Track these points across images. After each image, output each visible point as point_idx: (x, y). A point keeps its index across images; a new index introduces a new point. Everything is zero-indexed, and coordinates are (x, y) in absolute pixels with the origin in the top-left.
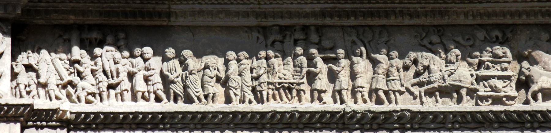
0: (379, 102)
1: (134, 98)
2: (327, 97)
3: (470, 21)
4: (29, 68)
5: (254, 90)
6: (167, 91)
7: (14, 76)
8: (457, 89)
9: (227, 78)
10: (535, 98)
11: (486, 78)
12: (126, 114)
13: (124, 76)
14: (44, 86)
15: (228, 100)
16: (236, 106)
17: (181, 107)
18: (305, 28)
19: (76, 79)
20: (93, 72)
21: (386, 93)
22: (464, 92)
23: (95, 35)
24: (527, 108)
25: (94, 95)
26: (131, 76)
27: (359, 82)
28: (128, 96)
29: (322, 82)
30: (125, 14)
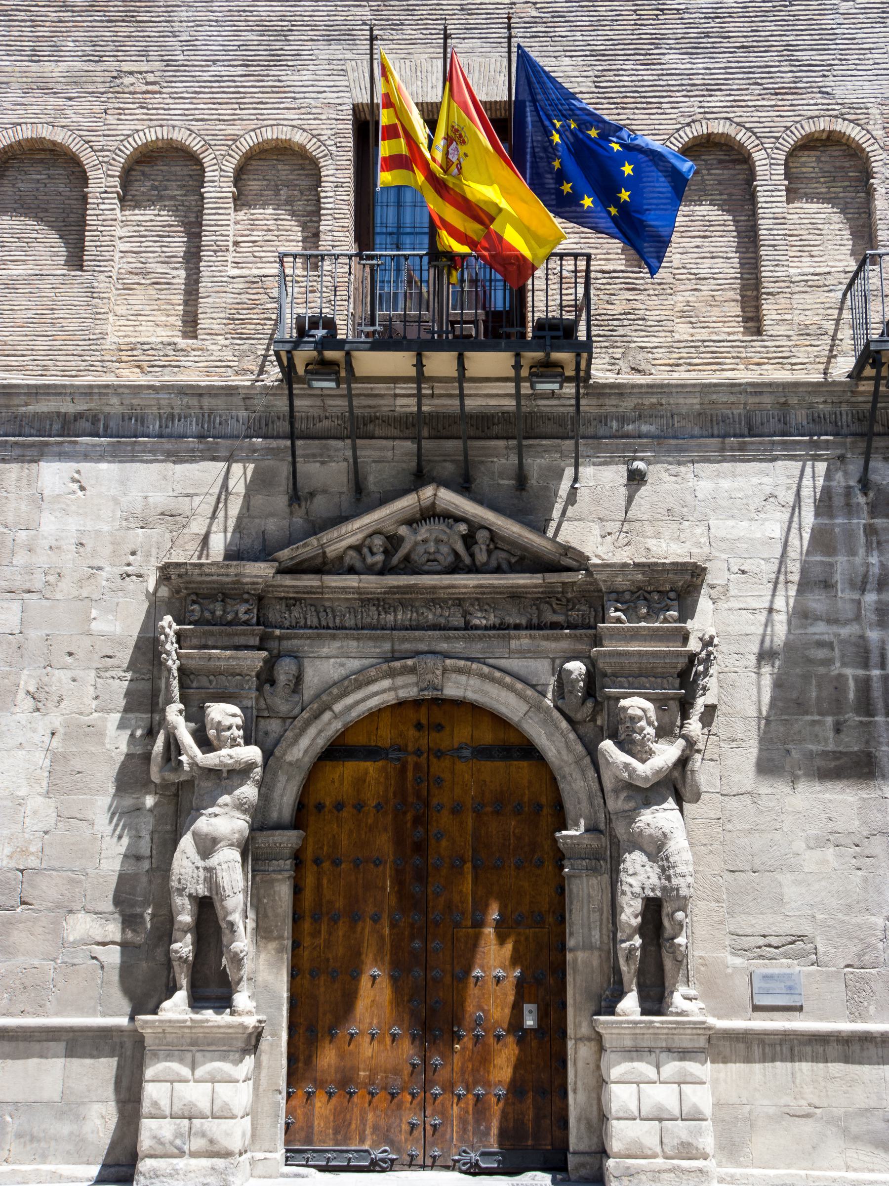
18: (378, 599)
30: (304, 593)
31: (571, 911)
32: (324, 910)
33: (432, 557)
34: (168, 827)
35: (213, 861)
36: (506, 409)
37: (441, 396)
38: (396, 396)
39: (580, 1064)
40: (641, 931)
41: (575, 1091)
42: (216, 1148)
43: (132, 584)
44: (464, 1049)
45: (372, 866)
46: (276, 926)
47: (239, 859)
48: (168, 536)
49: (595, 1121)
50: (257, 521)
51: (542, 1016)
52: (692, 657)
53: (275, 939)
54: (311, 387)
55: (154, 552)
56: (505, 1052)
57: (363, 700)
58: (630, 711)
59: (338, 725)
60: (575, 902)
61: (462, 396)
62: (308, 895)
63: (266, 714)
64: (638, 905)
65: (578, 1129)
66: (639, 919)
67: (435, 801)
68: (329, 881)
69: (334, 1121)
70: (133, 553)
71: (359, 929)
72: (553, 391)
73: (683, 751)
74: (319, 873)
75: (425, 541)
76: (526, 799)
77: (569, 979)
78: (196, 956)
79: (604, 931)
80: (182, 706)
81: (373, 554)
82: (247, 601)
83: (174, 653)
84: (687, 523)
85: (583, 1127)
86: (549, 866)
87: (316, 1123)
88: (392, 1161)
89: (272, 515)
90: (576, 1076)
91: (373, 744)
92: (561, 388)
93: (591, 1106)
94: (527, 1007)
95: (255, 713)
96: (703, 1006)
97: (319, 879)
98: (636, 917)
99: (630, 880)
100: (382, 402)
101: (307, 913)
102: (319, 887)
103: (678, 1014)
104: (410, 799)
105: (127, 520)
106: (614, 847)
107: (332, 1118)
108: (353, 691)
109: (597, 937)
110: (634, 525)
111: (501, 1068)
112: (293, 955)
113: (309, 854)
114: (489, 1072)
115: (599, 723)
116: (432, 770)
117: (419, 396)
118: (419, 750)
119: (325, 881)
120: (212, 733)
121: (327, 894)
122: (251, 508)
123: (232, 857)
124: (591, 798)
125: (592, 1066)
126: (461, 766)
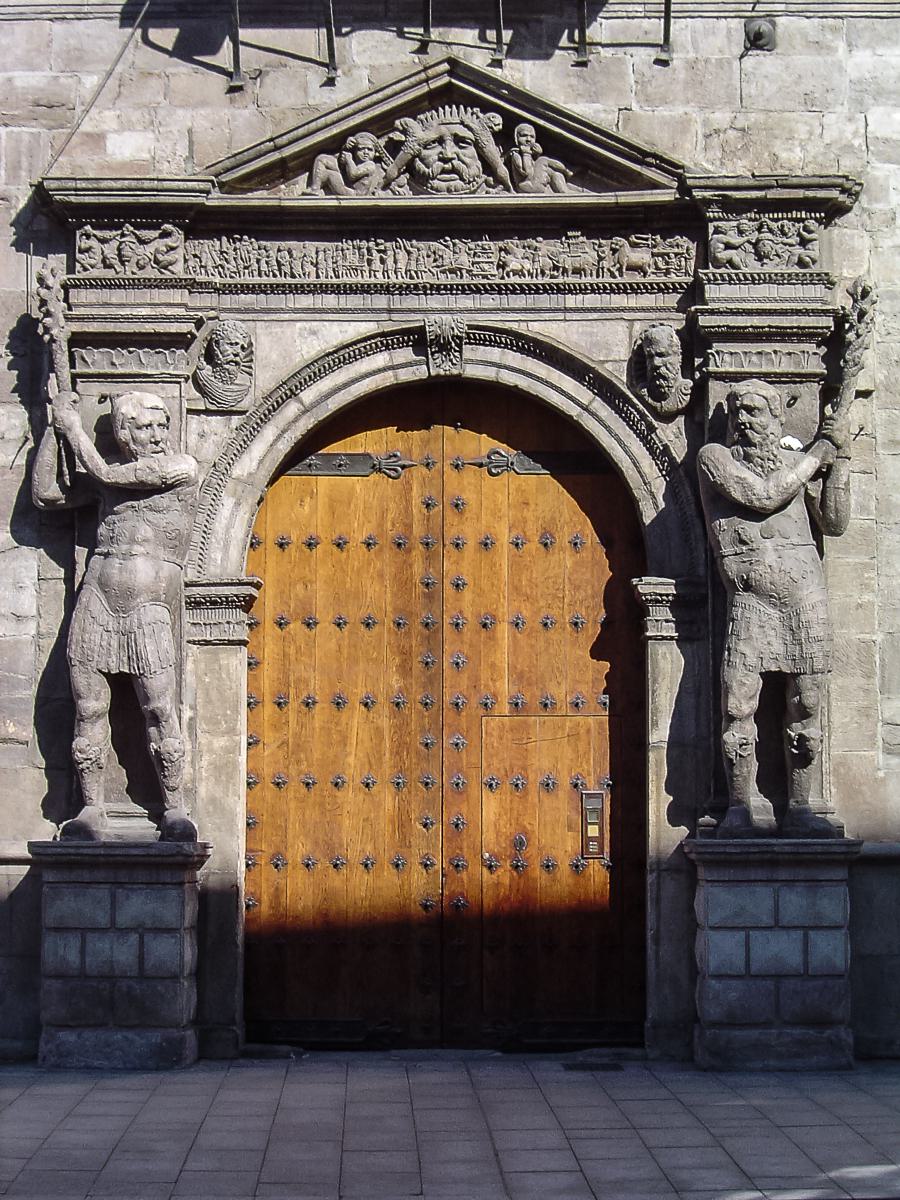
0: (411, 278)
1: (260, 275)
2: (379, 275)
3: (469, 227)
6: (280, 270)
7: (186, 261)
8: (460, 270)
9: (317, 263)
10: (508, 276)
11: (478, 263)
13: (253, 261)
14: (205, 267)
15: (318, 277)
16: (323, 280)
17: (289, 280)
20: (235, 259)
21: (416, 272)
22: (464, 272)
24: (503, 282)
25: (235, 273)
26: (258, 261)
27: (399, 265)
28: (256, 273)
29: (377, 265)
33: (448, 166)
40: (759, 716)
41: (657, 941)
46: (226, 715)
52: (841, 319)
53: (223, 734)
55: (25, 164)
57: (346, 385)
62: (268, 673)
64: (755, 683)
67: (451, 534)
73: (823, 459)
75: (441, 141)
81: (358, 161)
82: (166, 235)
84: (833, 116)
89: (204, 103)
90: (658, 917)
120: (124, 435)
123: (158, 617)
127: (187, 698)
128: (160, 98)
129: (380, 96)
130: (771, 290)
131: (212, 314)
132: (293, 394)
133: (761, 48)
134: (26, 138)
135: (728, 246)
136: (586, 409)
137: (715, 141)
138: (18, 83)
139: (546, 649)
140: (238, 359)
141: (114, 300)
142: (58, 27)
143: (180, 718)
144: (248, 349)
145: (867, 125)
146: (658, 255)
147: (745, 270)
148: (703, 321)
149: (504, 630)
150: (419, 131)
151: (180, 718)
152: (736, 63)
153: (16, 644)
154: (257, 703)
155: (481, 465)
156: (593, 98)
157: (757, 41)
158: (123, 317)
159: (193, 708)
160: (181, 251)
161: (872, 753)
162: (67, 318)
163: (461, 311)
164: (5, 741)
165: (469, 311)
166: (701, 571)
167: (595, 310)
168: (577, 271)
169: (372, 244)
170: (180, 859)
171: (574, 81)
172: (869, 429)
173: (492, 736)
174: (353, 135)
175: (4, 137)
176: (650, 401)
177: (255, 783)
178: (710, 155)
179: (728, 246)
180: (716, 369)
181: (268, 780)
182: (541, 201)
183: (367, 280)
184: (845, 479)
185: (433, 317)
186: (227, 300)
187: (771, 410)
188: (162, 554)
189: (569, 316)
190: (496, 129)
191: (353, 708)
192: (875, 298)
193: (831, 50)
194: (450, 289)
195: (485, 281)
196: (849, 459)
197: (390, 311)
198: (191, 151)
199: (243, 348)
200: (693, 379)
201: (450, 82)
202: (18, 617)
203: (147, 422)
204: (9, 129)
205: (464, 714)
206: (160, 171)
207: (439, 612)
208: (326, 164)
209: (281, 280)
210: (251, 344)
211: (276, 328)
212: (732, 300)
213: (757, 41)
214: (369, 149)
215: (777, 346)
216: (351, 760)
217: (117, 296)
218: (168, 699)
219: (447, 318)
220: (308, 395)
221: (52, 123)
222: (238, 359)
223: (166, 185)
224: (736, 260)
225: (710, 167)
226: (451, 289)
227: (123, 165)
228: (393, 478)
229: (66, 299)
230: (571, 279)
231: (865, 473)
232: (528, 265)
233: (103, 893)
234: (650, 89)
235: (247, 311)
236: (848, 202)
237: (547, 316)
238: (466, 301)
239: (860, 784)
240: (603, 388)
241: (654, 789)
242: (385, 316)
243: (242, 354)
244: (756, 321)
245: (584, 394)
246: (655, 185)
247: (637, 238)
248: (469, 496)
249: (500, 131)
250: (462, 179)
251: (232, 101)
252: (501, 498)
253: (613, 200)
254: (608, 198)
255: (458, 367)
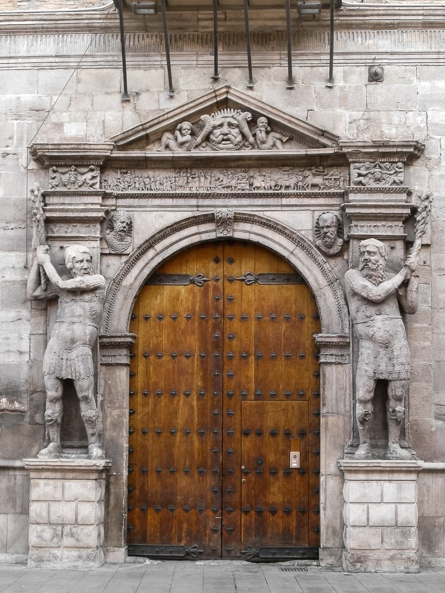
4: (105, 180)
5: (171, 187)
6: (145, 187)
7: (101, 183)
8: (231, 186)
10: (254, 189)
11: (240, 183)
12: (133, 194)
19: (119, 184)
22: (233, 187)
23: (125, 171)
31: (324, 389)
32: (151, 389)
33: (226, 137)
34: (41, 332)
35: (73, 354)
36: (279, 29)
37: (230, 20)
38: (199, 20)
39: (329, 492)
40: (373, 400)
41: (325, 509)
42: (81, 544)
43: (9, 161)
44: (248, 481)
45: (184, 359)
46: (118, 399)
47: (90, 353)
48: (35, 126)
49: (338, 528)
50: (99, 113)
51: (304, 459)
52: (414, 210)
53: (117, 408)
54: (136, 14)
56: (277, 484)
58: (368, 249)
59: (159, 259)
60: (327, 383)
61: (247, 20)
63: (107, 251)
64: (372, 384)
65: (327, 533)
66: (372, 394)
68: (154, 368)
69: (161, 528)
70: (10, 138)
71: (175, 402)
72: (314, 15)
73: (406, 277)
74: (147, 363)
75: (221, 125)
76: (293, 311)
77: (322, 435)
78: (63, 419)
79: (347, 403)
80: (47, 247)
81: (183, 135)
82: (92, 170)
83: (41, 209)
85: (330, 532)
86: (309, 359)
87: (148, 529)
88: (200, 553)
89: (110, 108)
91: (184, 273)
92: (320, 12)
93: (336, 518)
94: (292, 454)
95: (99, 251)
96: (415, 453)
97: (147, 367)
98: (370, 392)
99: (365, 367)
100: (188, 24)
101: (140, 390)
102: (147, 373)
103: (397, 458)
104: (211, 312)
105: (6, 114)
106: (355, 345)
107: (159, 526)
108: (170, 234)
109: (342, 407)
110: (372, 114)
111: (274, 494)
112: (130, 420)
113: (140, 350)
114: (266, 497)
115: (345, 257)
116: (226, 291)
117: (215, 19)
118: (216, 276)
119: (151, 368)
121: (153, 379)
122: (94, 104)
124: (339, 310)
125: (337, 492)
126: (246, 288)
127: (101, 390)
128: (90, 106)
129: (193, 104)
130: (381, 196)
131: (114, 208)
132: (151, 246)
133: (376, 81)
134: (26, 125)
135: (360, 175)
136: (292, 253)
137: (354, 125)
138: (22, 100)
139: (273, 368)
140: (125, 229)
141: (66, 202)
142: (41, 73)
143: (96, 401)
144: (130, 225)
145: (427, 117)
146: (326, 179)
147: (368, 186)
148: (348, 211)
149: (252, 358)
150: (210, 120)
151: (96, 401)
152: (365, 88)
153: (19, 366)
154: (134, 394)
155: (243, 280)
156: (296, 104)
157: (375, 77)
158: (70, 209)
159: (103, 395)
160: (98, 178)
161: (430, 419)
162: (44, 210)
163: (232, 206)
164: (2, 410)
165: (236, 206)
166: (347, 330)
167: (296, 206)
168: (287, 187)
169: (189, 175)
170: (95, 468)
171: (286, 97)
172: (428, 263)
173: (246, 410)
174: (181, 123)
175: (15, 125)
176: (323, 249)
177: (133, 432)
178: (351, 132)
179: (360, 175)
180: (354, 234)
181: (140, 431)
182: (270, 154)
183: (187, 191)
184: (416, 286)
185: (218, 209)
186: (121, 202)
187: (380, 253)
188: (89, 322)
189: (284, 209)
190: (249, 119)
191: (179, 396)
192: (431, 200)
193: (410, 82)
194: (226, 196)
195: (244, 192)
196: (418, 277)
197: (198, 206)
198: (104, 131)
199: (127, 224)
200: (343, 239)
201: (227, 99)
202: (21, 353)
203: (81, 259)
204: (18, 121)
205: (233, 399)
206: (89, 141)
207: (222, 351)
208: (167, 137)
209: (146, 192)
210: (131, 222)
211: (144, 215)
212: (363, 201)
213: (375, 77)
214: (188, 130)
215: (384, 223)
216: (179, 420)
217: (67, 200)
218: (90, 392)
219: (224, 209)
220: (159, 247)
221: (39, 118)
222: (125, 229)
223: (92, 147)
224: (364, 181)
225: (352, 138)
226: (227, 196)
227: (72, 138)
228: (200, 286)
229: (44, 201)
230: (283, 191)
231: (426, 283)
232: (263, 184)
233: (59, 483)
234: (323, 101)
235: (130, 207)
236: (419, 154)
237: (273, 209)
238: (234, 202)
239: (424, 434)
240: (299, 242)
241: (324, 436)
242: (195, 209)
243: (127, 227)
244: (373, 211)
245: (291, 246)
246: (325, 146)
247: (316, 171)
248: (237, 295)
249: (251, 120)
250: (232, 143)
251: (123, 107)
252: (251, 296)
253: (305, 153)
254: (302, 151)
255: (231, 232)
